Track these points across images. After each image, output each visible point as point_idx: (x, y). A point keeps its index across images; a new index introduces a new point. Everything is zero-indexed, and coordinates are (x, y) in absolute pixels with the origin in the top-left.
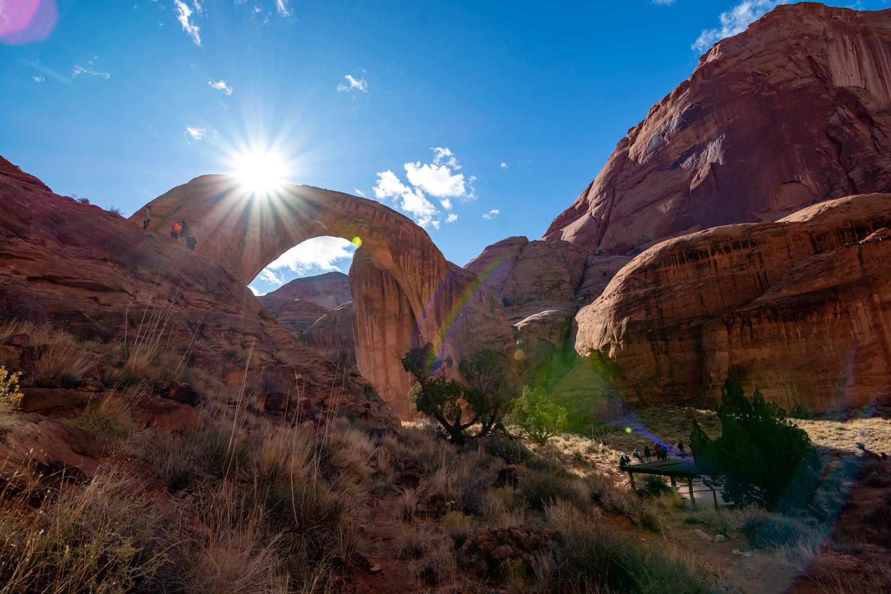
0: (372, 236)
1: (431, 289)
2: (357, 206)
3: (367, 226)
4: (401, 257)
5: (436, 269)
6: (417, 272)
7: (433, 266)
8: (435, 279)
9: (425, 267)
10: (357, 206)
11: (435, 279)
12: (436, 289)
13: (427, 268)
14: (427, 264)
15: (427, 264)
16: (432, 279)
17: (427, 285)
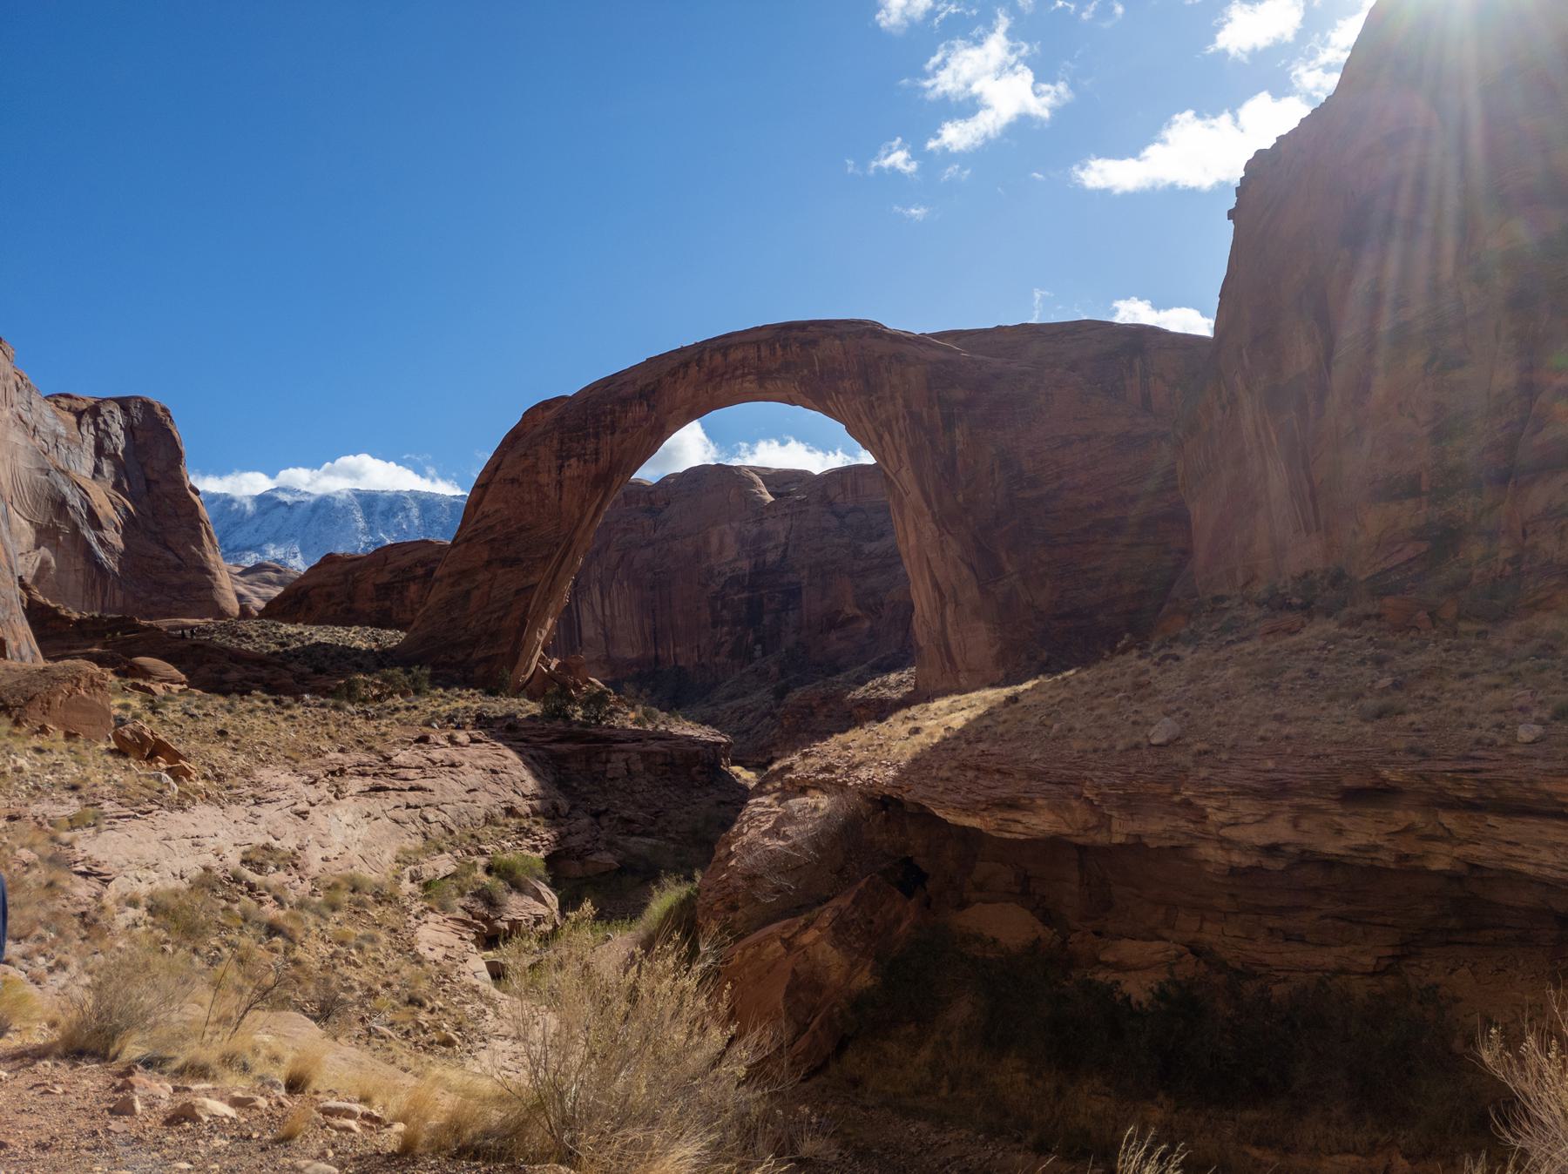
0: (766, 388)
1: (897, 441)
2: (725, 355)
3: (751, 377)
4: (829, 403)
5: (900, 401)
6: (864, 418)
7: (893, 398)
8: (901, 421)
9: (876, 404)
10: (725, 355)
11: (901, 421)
12: (907, 441)
13: (880, 406)
14: (878, 399)
15: (878, 399)
16: (894, 423)
17: (887, 437)
